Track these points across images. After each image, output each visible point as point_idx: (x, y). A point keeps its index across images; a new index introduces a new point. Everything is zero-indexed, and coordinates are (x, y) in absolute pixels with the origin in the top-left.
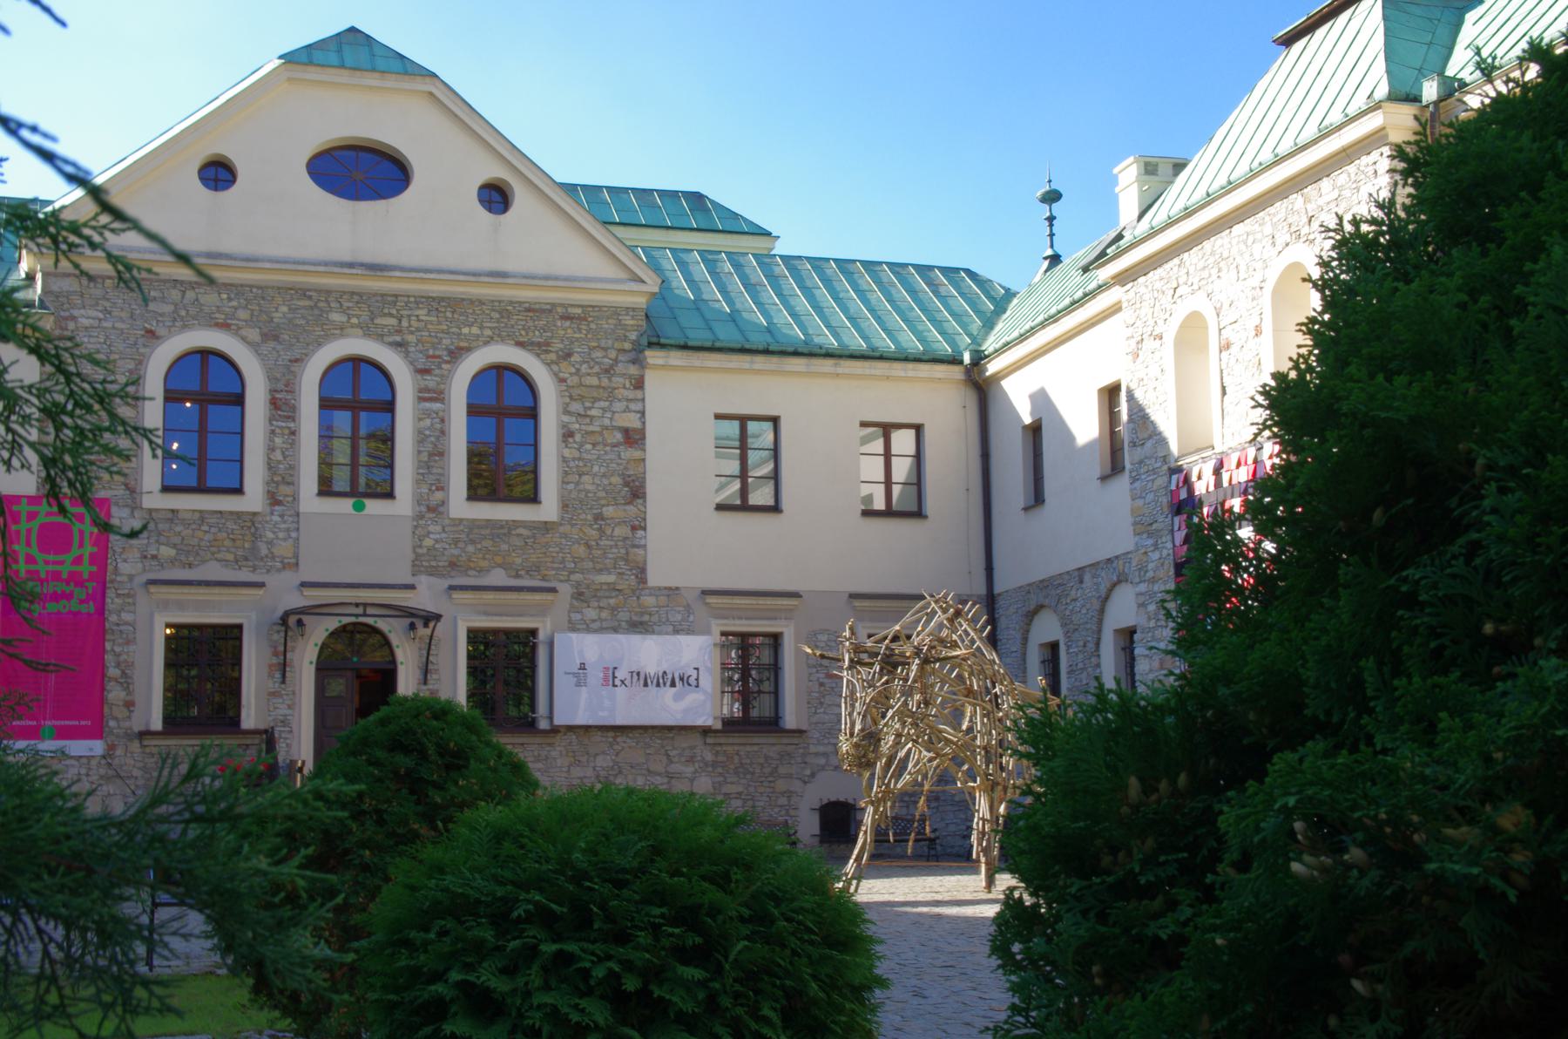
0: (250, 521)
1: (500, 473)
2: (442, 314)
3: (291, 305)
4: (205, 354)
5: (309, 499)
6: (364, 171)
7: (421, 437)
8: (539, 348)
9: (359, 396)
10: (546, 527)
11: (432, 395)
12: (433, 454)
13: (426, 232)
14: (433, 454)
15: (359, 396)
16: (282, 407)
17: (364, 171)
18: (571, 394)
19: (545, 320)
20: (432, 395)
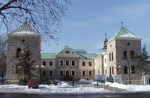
0: (63, 67)
1: (73, 64)
2: (70, 58)
3: (65, 58)
4: (61, 60)
5: (66, 66)
6: (67, 52)
7: (70, 63)
8: (75, 59)
9: (67, 62)
10: (75, 67)
11: (70, 61)
12: (70, 64)
13: (70, 55)
14: (70, 64)
15: (67, 62)
16: (64, 62)
17: (67, 52)
18: (76, 61)
19: (75, 58)
20: (70, 61)
